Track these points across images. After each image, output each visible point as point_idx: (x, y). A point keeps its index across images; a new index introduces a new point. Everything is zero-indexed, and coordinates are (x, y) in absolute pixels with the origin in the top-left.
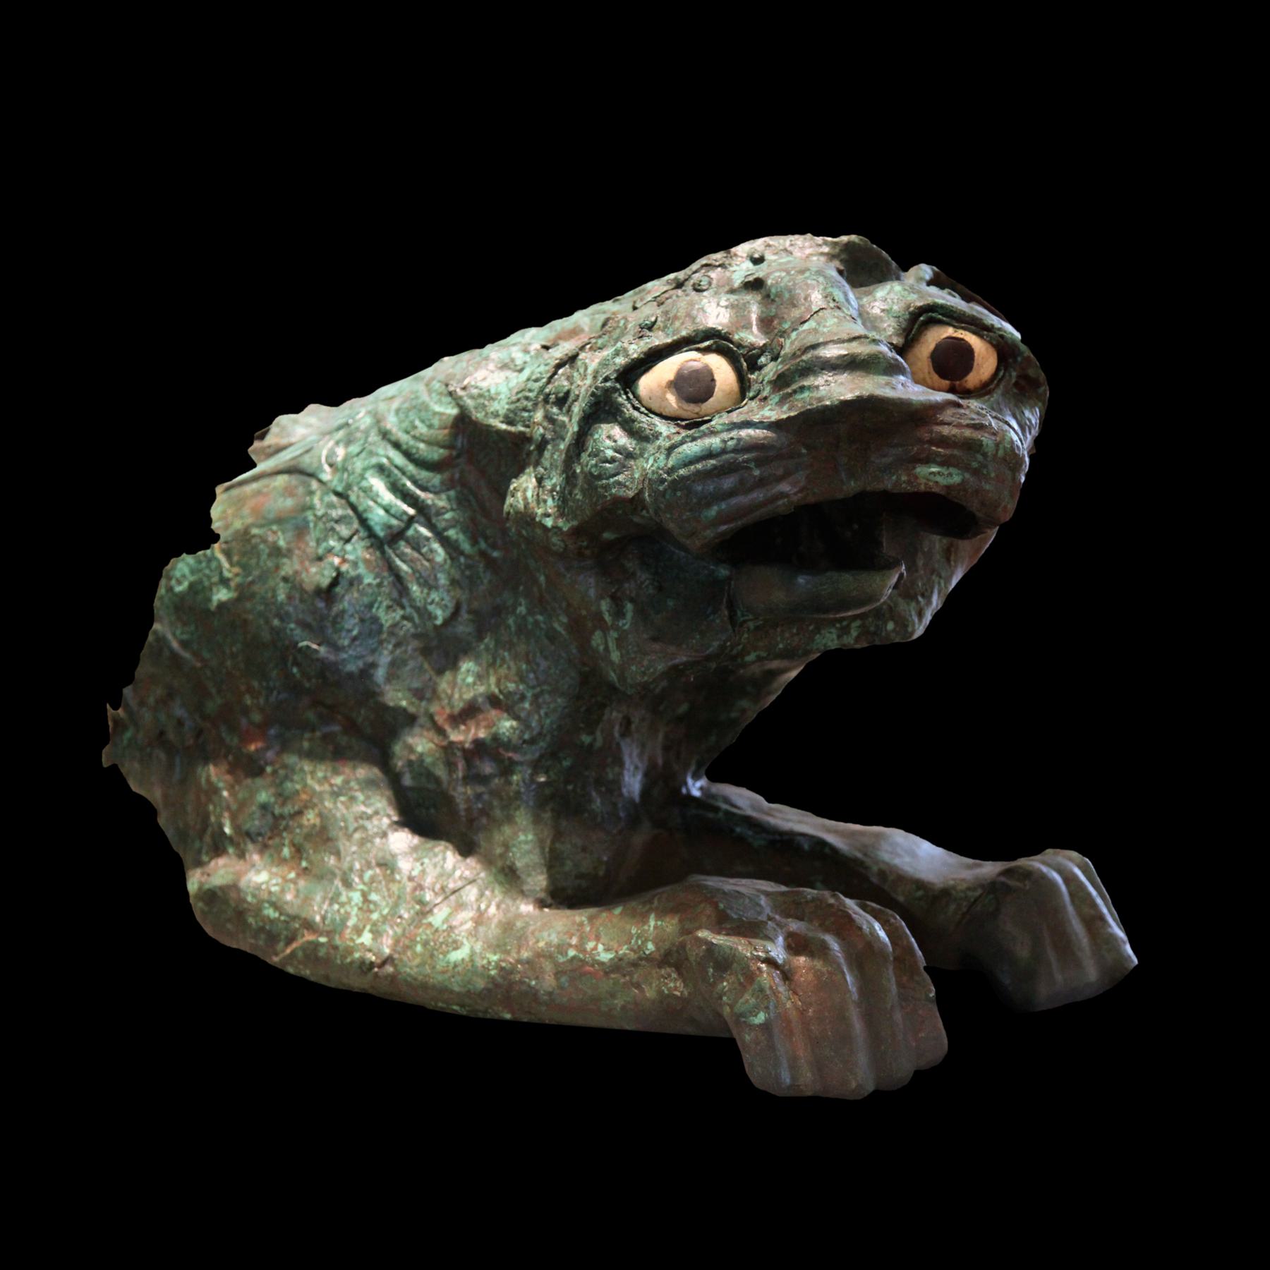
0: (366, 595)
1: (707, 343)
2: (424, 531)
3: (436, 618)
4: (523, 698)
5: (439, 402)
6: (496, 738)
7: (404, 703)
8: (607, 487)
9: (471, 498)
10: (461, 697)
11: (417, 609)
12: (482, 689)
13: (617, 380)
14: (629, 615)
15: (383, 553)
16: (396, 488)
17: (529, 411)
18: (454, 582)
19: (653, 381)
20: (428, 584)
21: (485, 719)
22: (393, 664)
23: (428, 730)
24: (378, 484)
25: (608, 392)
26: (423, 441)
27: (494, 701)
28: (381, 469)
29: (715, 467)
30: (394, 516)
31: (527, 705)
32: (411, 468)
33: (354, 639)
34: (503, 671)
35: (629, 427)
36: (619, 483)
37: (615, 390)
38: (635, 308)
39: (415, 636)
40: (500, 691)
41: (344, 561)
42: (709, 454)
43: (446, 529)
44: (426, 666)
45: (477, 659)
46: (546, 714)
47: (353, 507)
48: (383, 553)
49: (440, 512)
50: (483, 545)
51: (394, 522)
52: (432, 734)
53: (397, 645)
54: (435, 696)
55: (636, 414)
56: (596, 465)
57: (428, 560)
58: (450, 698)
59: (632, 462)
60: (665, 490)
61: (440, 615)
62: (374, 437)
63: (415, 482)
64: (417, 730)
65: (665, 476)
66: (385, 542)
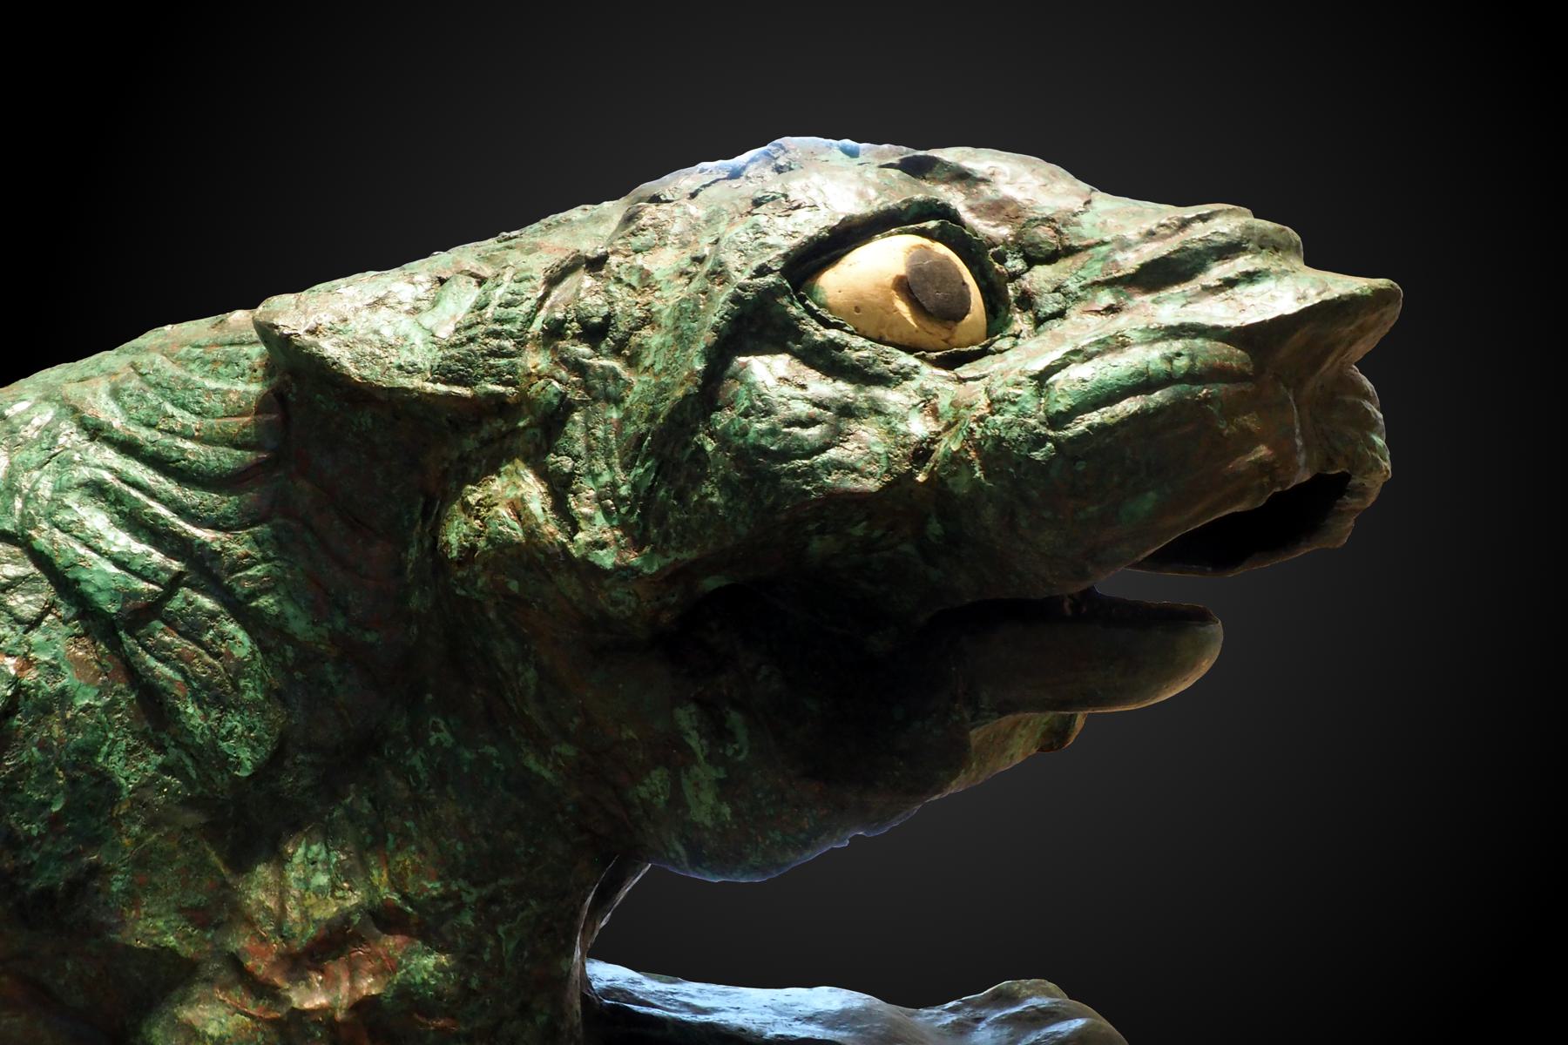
0: (83, 729)
1: (932, 224)
2: (208, 603)
3: (239, 764)
4: (459, 907)
5: (217, 376)
6: (405, 992)
7: (171, 940)
8: (811, 474)
9: (308, 537)
10: (305, 915)
11: (197, 754)
12: (354, 899)
13: (784, 272)
14: (742, 734)
15: (115, 645)
16: (135, 522)
17: (510, 355)
18: (269, 692)
19: (836, 282)
20: (215, 697)
21: (370, 957)
22: (141, 862)
23: (225, 988)
24: (97, 520)
25: (770, 293)
26: (192, 438)
27: (385, 919)
28: (96, 490)
29: (1160, 409)
30: (140, 575)
31: (467, 919)
32: (170, 487)
33: (55, 820)
34: (406, 859)
35: (827, 360)
36: (838, 465)
37: (784, 292)
38: (693, 195)
39: (189, 803)
40: (404, 897)
41: (28, 663)
42: (1144, 383)
43: (253, 595)
44: (214, 858)
45: (329, 835)
46: (509, 933)
47: (42, 560)
48: (115, 645)
49: (236, 567)
50: (340, 623)
51: (143, 586)
52: (237, 995)
53: (152, 824)
54: (238, 915)
55: (833, 333)
56: (773, 432)
57: (216, 656)
58: (280, 919)
59: (853, 426)
60: (1050, 461)
61: (246, 759)
62: (70, 435)
63: (181, 511)
64: (198, 990)
65: (1043, 430)
66: (109, 626)
